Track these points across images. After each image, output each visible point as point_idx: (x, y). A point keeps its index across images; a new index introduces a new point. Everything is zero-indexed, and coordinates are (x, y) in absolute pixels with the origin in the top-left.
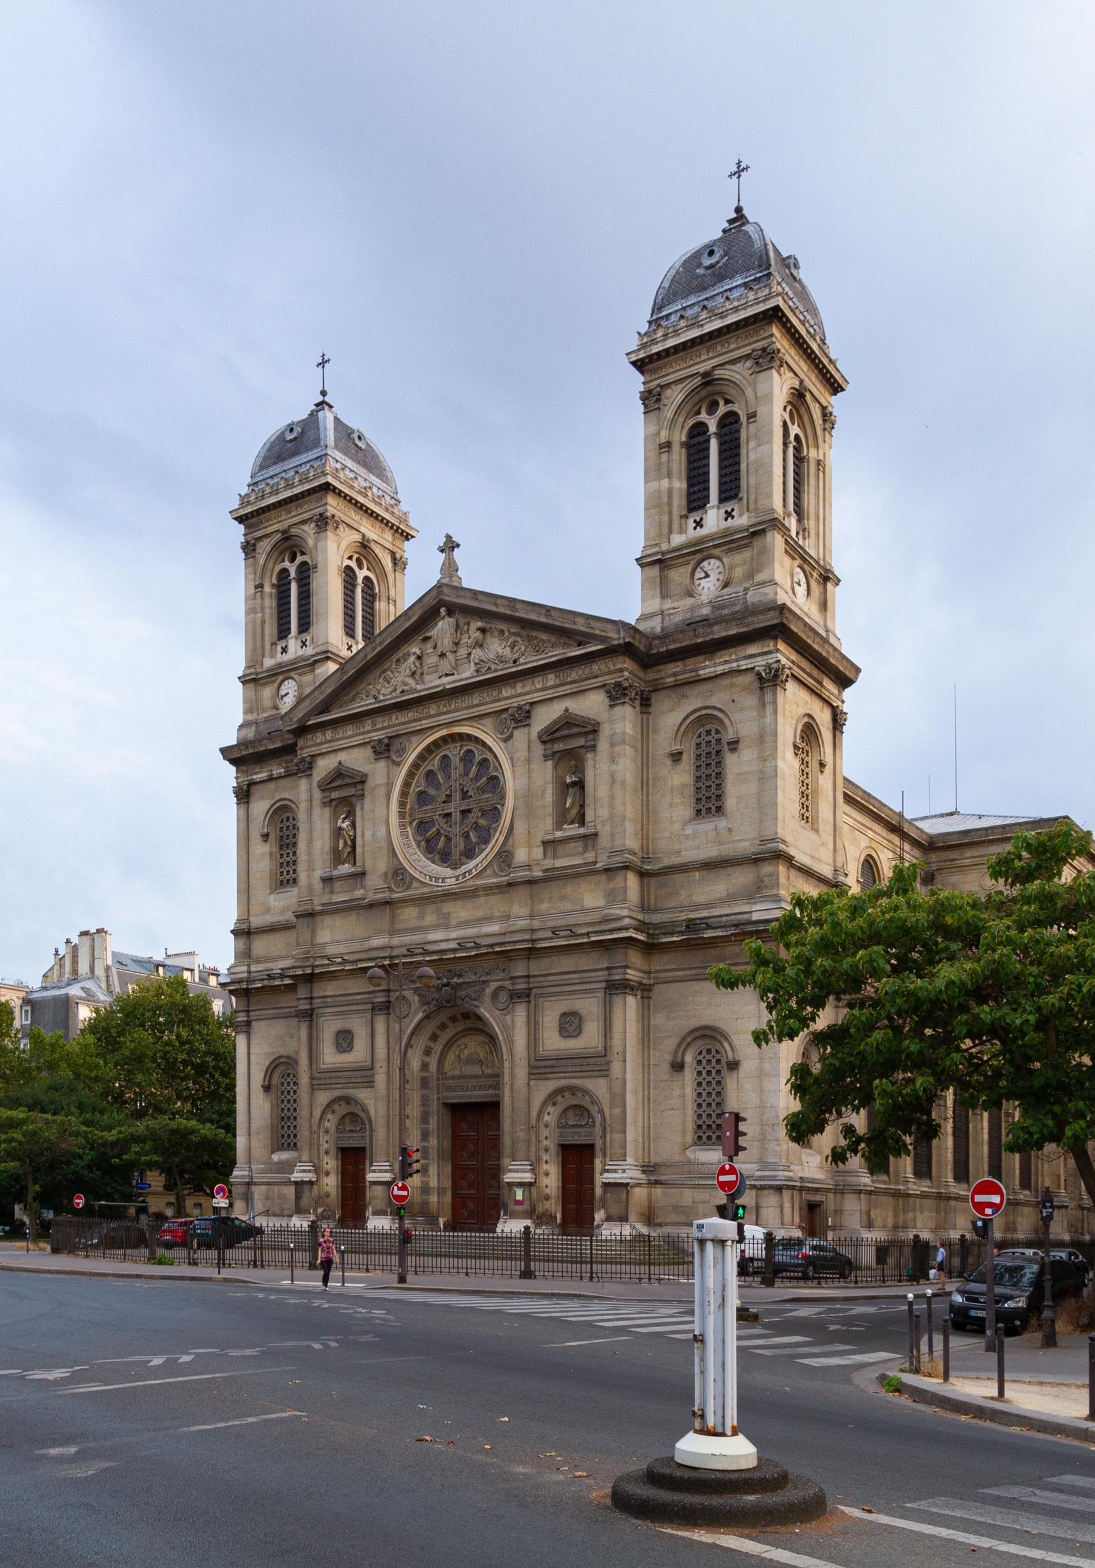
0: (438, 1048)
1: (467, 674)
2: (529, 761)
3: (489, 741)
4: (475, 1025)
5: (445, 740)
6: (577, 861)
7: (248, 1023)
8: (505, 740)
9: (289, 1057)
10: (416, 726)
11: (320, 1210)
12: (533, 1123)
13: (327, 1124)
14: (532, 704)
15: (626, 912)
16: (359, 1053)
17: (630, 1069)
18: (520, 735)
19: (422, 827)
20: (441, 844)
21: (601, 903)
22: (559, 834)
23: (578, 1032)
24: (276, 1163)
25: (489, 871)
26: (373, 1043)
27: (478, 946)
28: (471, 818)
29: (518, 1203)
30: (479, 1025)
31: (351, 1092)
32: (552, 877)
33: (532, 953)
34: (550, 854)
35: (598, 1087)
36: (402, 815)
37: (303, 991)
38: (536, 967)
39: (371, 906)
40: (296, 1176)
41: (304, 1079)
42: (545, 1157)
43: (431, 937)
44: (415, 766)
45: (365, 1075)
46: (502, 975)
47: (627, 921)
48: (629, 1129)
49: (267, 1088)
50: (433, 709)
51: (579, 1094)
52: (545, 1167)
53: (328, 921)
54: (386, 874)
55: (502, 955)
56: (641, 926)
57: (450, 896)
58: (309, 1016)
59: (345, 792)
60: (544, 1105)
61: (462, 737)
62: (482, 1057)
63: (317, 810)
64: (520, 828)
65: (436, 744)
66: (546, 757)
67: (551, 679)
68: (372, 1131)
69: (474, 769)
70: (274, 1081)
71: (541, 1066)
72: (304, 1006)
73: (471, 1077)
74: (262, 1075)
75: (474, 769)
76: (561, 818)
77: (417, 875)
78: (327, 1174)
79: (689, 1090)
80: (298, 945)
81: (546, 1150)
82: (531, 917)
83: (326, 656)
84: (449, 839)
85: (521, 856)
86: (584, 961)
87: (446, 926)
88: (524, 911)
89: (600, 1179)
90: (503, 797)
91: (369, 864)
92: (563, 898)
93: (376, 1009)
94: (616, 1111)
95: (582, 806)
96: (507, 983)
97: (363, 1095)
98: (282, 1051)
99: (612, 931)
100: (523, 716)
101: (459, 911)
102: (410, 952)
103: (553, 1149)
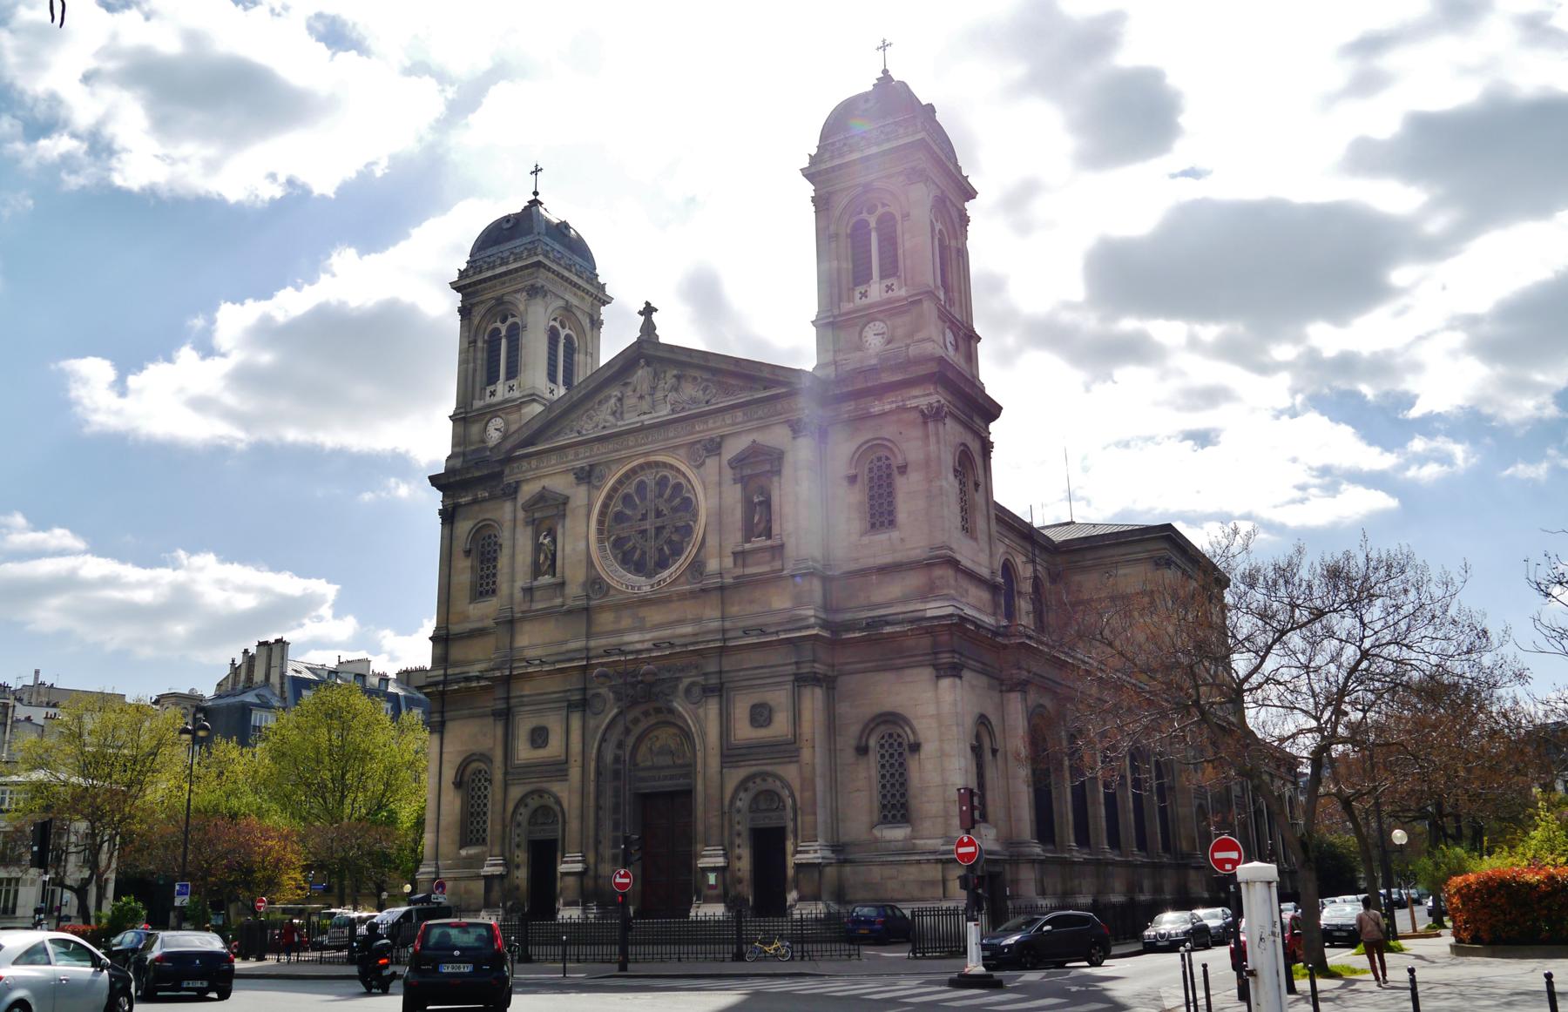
0: (631, 741)
1: (664, 412)
2: (720, 484)
3: (683, 468)
4: (668, 717)
5: (642, 467)
6: (765, 568)
7: (443, 724)
8: (698, 467)
9: (482, 755)
10: (616, 456)
11: (509, 904)
12: (726, 808)
13: (519, 818)
14: (722, 437)
15: (811, 612)
16: (554, 748)
17: (813, 754)
18: (712, 463)
19: (618, 543)
20: (636, 556)
21: (788, 605)
22: (747, 546)
23: (768, 722)
25: (682, 579)
26: (566, 738)
27: (672, 645)
28: (666, 534)
29: (712, 887)
30: (670, 718)
31: (545, 785)
32: (742, 583)
33: (723, 651)
34: (740, 562)
35: (790, 772)
36: (600, 531)
37: (500, 693)
38: (728, 663)
39: (570, 612)
40: (487, 870)
41: (498, 775)
42: (738, 841)
43: (627, 638)
44: (614, 489)
45: (558, 769)
46: (694, 672)
47: (812, 620)
48: (819, 811)
49: (458, 784)
50: (631, 441)
51: (770, 780)
52: (738, 851)
53: (527, 627)
54: (584, 584)
55: (693, 655)
56: (825, 625)
57: (645, 602)
58: (506, 716)
59: (547, 514)
60: (737, 790)
61: (657, 464)
62: (673, 746)
63: (520, 529)
64: (712, 542)
65: (634, 471)
66: (735, 481)
67: (739, 414)
68: (564, 822)
69: (668, 491)
70: (466, 778)
71: (731, 754)
72: (501, 705)
73: (662, 768)
74: (453, 773)
75: (668, 491)
76: (749, 532)
77: (613, 584)
78: (518, 867)
79: (874, 772)
80: (497, 649)
81: (739, 835)
82: (723, 618)
83: (533, 398)
84: (644, 553)
85: (713, 565)
86: (775, 657)
87: (642, 629)
88: (717, 614)
89: (791, 861)
90: (695, 515)
91: (568, 574)
92: (751, 602)
93: (571, 706)
94: (807, 794)
95: (769, 521)
96: (700, 679)
97: (557, 788)
98: (475, 748)
99: (800, 629)
100: (714, 447)
101: (654, 616)
102: (607, 653)
103: (745, 834)
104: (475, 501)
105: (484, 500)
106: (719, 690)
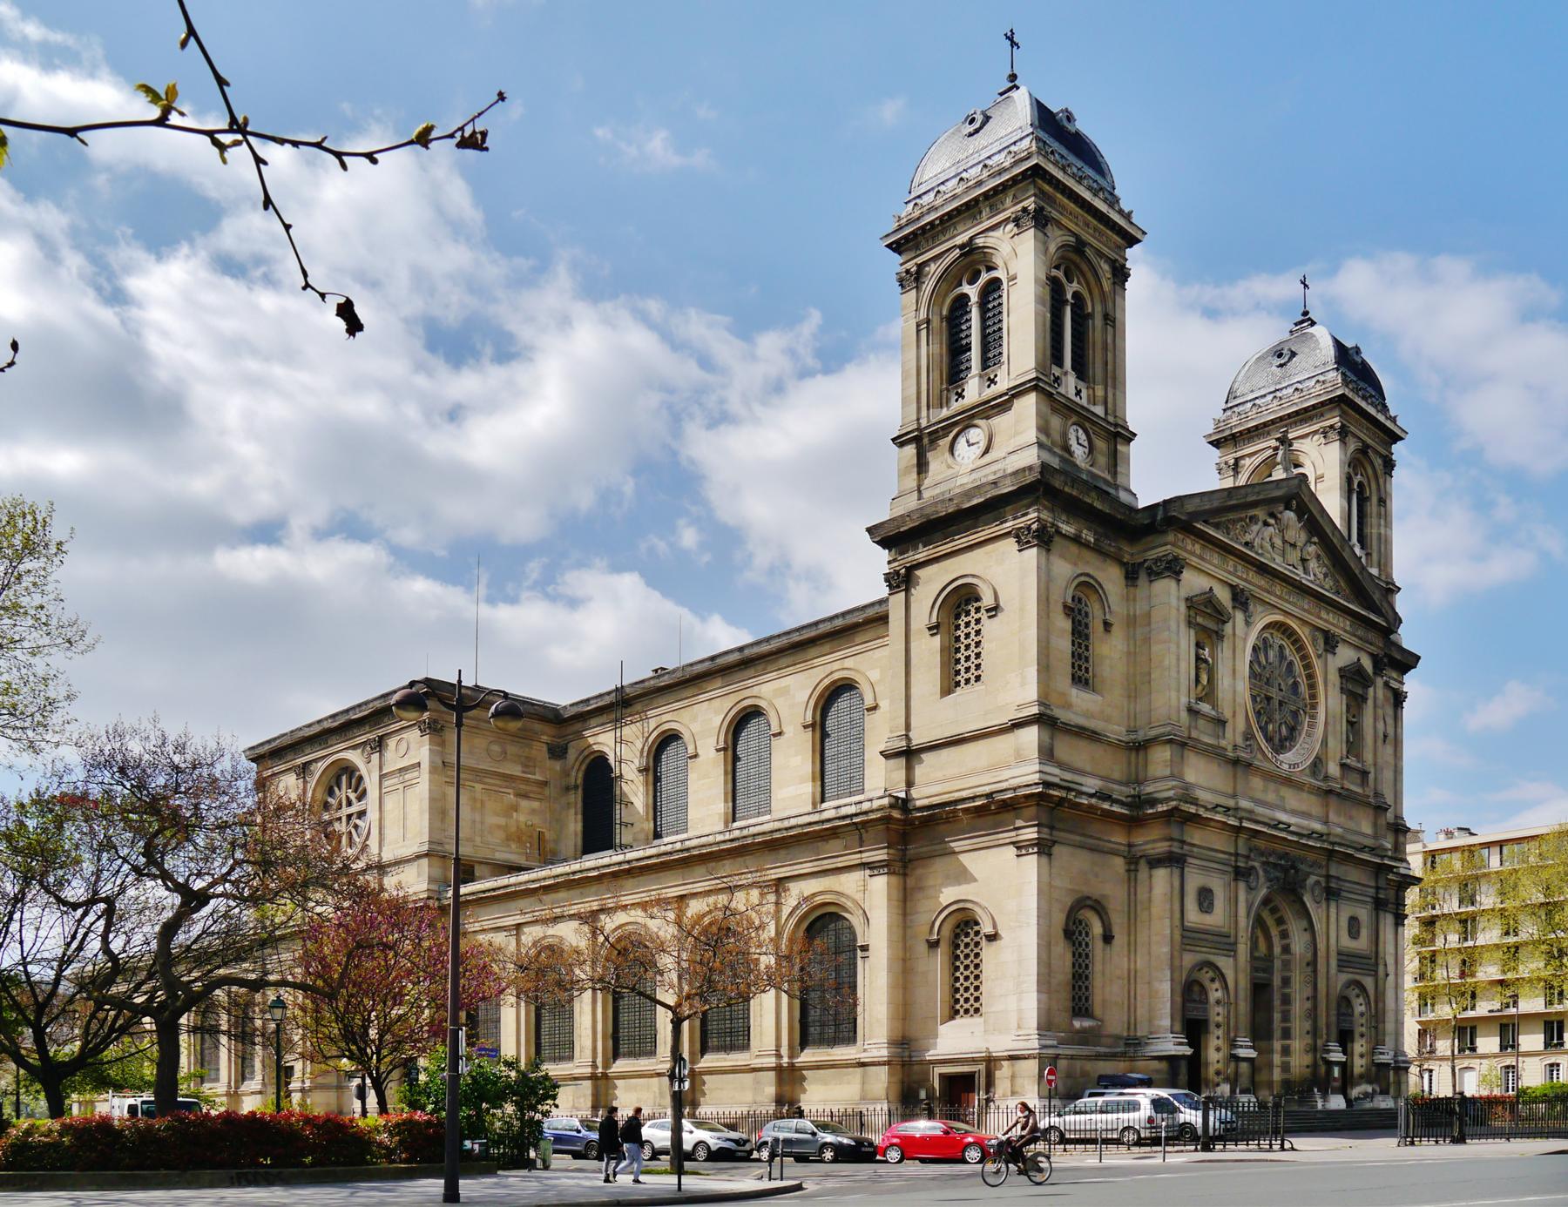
9: (1096, 901)
16: (1216, 919)
24: (1078, 1032)
57: (1288, 781)
87: (1285, 810)
91: (1227, 714)
92: (1351, 818)
98: (1086, 891)
104: (1076, 539)
105: (1086, 545)
106: (1331, 894)
